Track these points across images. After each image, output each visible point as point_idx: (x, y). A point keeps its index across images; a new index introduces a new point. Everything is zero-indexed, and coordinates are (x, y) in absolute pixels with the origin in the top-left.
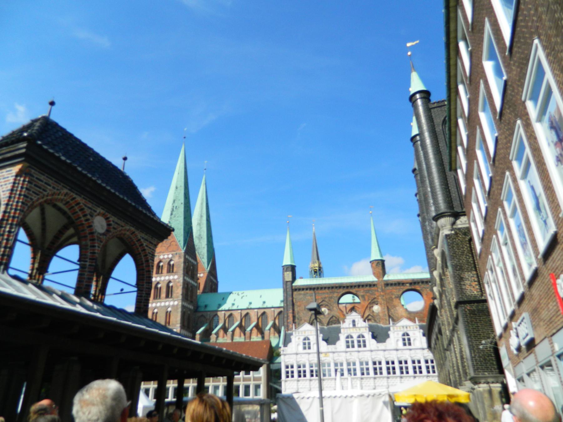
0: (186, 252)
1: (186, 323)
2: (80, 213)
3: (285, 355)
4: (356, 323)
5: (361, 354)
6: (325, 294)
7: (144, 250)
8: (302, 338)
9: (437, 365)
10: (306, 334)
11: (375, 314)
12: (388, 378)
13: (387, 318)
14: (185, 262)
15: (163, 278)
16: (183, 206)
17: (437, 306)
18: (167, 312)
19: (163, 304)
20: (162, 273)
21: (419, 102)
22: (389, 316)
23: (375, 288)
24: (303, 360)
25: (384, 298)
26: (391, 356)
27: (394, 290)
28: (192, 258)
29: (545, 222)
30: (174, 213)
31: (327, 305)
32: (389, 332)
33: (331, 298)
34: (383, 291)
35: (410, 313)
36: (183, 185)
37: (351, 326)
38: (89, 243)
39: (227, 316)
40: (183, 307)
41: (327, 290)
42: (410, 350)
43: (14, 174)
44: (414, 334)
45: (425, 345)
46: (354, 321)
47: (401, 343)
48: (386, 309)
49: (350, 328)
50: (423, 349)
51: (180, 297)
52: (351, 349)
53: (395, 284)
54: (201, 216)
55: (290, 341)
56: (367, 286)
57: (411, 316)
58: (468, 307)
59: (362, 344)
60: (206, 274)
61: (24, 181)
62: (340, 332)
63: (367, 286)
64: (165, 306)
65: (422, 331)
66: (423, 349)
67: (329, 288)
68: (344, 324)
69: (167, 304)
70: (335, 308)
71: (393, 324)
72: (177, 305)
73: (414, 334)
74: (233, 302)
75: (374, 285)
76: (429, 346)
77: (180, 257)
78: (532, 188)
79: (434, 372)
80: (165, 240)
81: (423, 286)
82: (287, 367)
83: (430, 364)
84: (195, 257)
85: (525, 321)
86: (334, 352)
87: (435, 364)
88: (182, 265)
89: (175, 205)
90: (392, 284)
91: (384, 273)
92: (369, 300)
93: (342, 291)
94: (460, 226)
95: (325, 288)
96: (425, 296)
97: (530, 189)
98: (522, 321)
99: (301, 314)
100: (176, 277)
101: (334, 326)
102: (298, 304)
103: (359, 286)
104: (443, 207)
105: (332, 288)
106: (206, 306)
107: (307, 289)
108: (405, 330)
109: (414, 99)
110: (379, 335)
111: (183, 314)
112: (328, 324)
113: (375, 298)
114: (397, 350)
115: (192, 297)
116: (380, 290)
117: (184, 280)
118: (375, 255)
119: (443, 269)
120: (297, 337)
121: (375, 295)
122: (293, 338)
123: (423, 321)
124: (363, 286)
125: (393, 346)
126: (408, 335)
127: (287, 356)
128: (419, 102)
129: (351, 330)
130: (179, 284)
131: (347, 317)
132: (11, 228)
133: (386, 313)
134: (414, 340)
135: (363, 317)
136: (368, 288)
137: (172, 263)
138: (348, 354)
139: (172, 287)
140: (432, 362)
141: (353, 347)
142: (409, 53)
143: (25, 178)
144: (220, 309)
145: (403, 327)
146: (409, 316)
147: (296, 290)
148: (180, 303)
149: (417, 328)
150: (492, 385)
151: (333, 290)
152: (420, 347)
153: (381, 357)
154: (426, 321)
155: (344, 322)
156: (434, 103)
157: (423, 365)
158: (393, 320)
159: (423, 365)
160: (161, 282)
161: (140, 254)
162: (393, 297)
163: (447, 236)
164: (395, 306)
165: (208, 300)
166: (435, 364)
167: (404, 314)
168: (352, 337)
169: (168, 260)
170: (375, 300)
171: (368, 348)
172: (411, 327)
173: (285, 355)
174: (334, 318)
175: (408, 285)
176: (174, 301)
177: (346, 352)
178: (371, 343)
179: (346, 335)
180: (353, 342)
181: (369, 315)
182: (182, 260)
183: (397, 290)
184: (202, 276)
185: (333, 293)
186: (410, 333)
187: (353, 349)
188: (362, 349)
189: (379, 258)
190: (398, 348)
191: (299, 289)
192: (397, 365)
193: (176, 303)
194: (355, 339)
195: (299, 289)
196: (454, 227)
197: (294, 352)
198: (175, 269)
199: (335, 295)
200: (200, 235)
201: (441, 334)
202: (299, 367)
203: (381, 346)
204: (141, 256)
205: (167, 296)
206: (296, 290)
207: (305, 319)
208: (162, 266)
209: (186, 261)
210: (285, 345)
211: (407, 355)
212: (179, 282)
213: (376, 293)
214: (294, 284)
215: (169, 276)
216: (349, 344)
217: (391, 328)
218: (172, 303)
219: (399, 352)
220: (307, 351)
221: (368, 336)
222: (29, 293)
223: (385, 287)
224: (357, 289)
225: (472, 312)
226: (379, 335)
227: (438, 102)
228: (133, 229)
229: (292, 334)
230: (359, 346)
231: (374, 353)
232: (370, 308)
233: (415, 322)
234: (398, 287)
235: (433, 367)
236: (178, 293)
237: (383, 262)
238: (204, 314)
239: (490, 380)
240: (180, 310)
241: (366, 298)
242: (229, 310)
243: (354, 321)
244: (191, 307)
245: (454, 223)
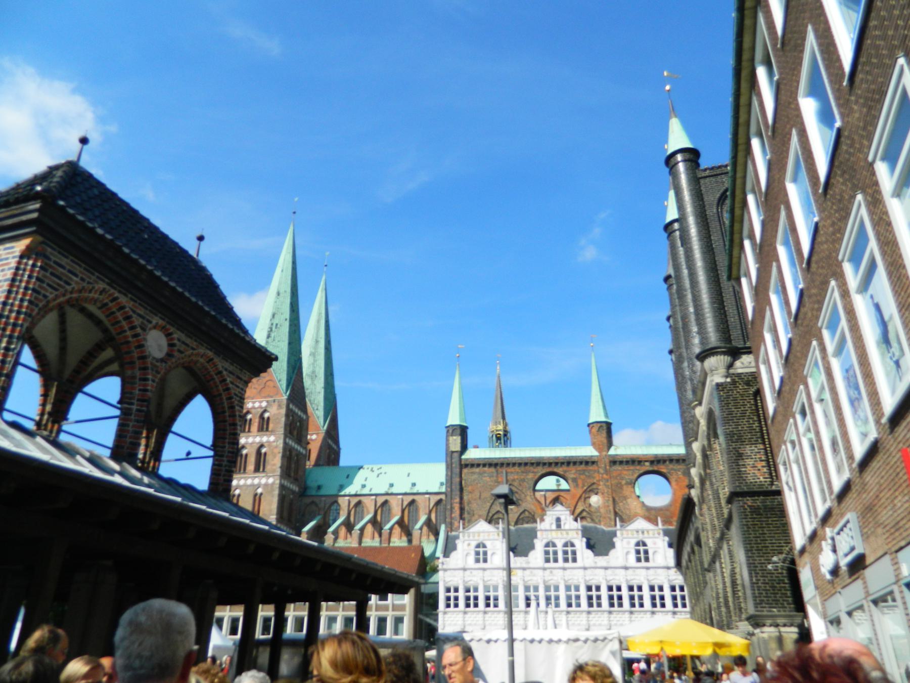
0: (291, 399)
1: (285, 514)
2: (124, 323)
3: (445, 570)
4: (562, 523)
5: (568, 572)
6: (515, 474)
7: (228, 389)
8: (474, 544)
9: (691, 594)
10: (481, 539)
11: (593, 510)
12: (610, 612)
13: (613, 517)
14: (287, 416)
15: (250, 440)
16: (287, 324)
17: (696, 500)
18: (256, 495)
19: (249, 482)
20: (249, 431)
21: (681, 167)
22: (616, 514)
23: (594, 467)
24: (475, 579)
25: (609, 484)
26: (617, 578)
27: (625, 472)
28: (300, 409)
29: (897, 363)
30: (272, 335)
32: (615, 540)
33: (523, 480)
34: (606, 472)
35: (649, 509)
36: (289, 290)
37: (554, 527)
38: (138, 373)
39: (352, 504)
40: (282, 487)
41: (516, 468)
42: (648, 568)
43: (18, 254)
44: (655, 544)
45: (671, 562)
46: (558, 520)
47: (632, 557)
48: (611, 503)
49: (551, 530)
50: (669, 568)
51: (278, 472)
52: (552, 564)
53: (627, 462)
54: (317, 342)
55: (454, 548)
56: (581, 463)
57: (651, 515)
58: (749, 501)
59: (571, 556)
60: (322, 436)
61: (34, 266)
62: (536, 537)
63: (581, 463)
64: (252, 485)
65: (667, 539)
66: (669, 568)
67: (520, 464)
68: (543, 524)
69: (256, 481)
70: (528, 498)
71: (621, 526)
72: (273, 483)
73: (655, 544)
74: (364, 483)
75: (593, 463)
76: (678, 564)
77: (280, 406)
78: (877, 307)
79: (684, 606)
80: (262, 375)
81: (671, 466)
82: (448, 590)
83: (678, 593)
84: (304, 409)
85: (849, 526)
86: (524, 569)
87: (686, 593)
88: (283, 419)
89: (275, 321)
90: (621, 462)
91: (610, 444)
92: (584, 486)
93: (541, 470)
94: (740, 371)
95: (514, 464)
96: (674, 483)
97: (873, 309)
98: (845, 526)
99: (474, 506)
100: (272, 438)
101: (526, 526)
102: (470, 488)
103: (568, 463)
104: (713, 338)
105: (526, 464)
106: (319, 487)
107: (484, 465)
108: (640, 537)
109: (672, 161)
110: (599, 543)
111: (282, 499)
112: (516, 523)
113: (594, 484)
114: (626, 568)
115: (296, 471)
116: (601, 471)
117: (285, 443)
118: (597, 414)
119: (709, 440)
120: (466, 543)
121: (594, 478)
122: (459, 544)
123: (670, 524)
124: (575, 463)
125: (620, 562)
126: (644, 544)
127: (448, 573)
128: (681, 167)
129: (554, 534)
130: (276, 451)
131: (548, 513)
132: (9, 343)
133: (611, 508)
134: (655, 553)
135: (573, 513)
136: (583, 467)
137: (266, 415)
138: (548, 572)
139: (265, 454)
140: (682, 589)
141: (556, 560)
142: (668, 88)
143: (36, 261)
144: (342, 493)
145: (637, 532)
146: (647, 514)
147: (466, 466)
148: (278, 482)
149: (659, 534)
150: (783, 629)
151: (527, 467)
152: (663, 564)
153: (600, 578)
154: (675, 523)
155: (542, 520)
156: (705, 170)
157: (667, 593)
158: (622, 520)
159: (667, 593)
160: (247, 446)
161: (220, 395)
162: (624, 482)
163: (718, 385)
164: (625, 498)
165: (322, 479)
166: (686, 593)
167: (639, 510)
168: (554, 545)
169: (260, 411)
170: (594, 487)
171: (580, 563)
172: (651, 532)
173: (445, 570)
174: (527, 513)
175: (647, 464)
176: (268, 477)
177: (545, 569)
178: (585, 556)
179: (545, 541)
180: (555, 553)
181: (583, 510)
182: (283, 411)
183: (630, 472)
184: (315, 438)
185: (527, 472)
186: (648, 541)
187: (555, 565)
189: (603, 419)
190: (628, 565)
191: (472, 465)
192: (625, 593)
193: (271, 480)
194: (560, 549)
195: (472, 465)
196: (731, 371)
197: (461, 565)
198: (271, 426)
199: (530, 476)
200: (314, 372)
201: (700, 545)
202: (468, 591)
203: (601, 561)
204: (221, 399)
205: (257, 469)
206: (466, 466)
207: (481, 513)
208: (251, 420)
209: (289, 413)
210: (446, 554)
211: (641, 577)
212: (276, 447)
213: (596, 475)
214: (463, 457)
215: (261, 436)
217: (618, 533)
218: (264, 481)
219: (630, 571)
220: (482, 565)
221: (580, 544)
222: (36, 450)
223: (610, 466)
224: (565, 468)
225: (755, 510)
226: (599, 543)
227: (712, 168)
228: (210, 354)
229: (457, 537)
230: (566, 560)
231: (589, 572)
232: (585, 499)
233: (657, 525)
234: (632, 468)
235: (683, 598)
236: (274, 465)
237: (609, 425)
238: (317, 500)
239: (780, 621)
240: (276, 492)
241: (580, 482)
242: (356, 495)
243: (558, 520)
244: (295, 488)
245: (730, 366)
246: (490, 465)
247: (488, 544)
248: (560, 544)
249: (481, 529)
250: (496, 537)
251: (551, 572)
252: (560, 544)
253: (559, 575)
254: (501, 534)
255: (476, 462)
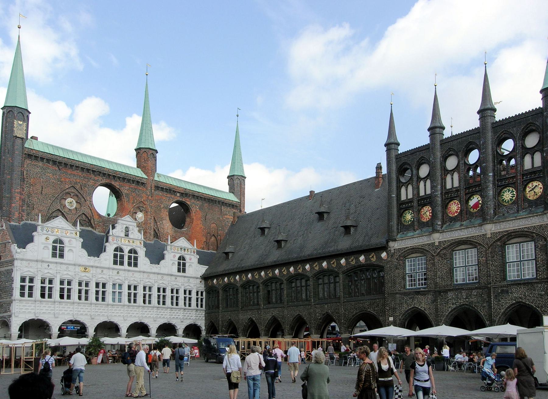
4: (130, 233)
8: (52, 239)
10: (59, 234)
31: (77, 196)
32: (165, 252)
37: (123, 235)
42: (185, 277)
46: (127, 230)
47: (176, 267)
50: (197, 278)
56: (133, 181)
59: (134, 262)
66: (197, 278)
67: (83, 169)
68: (114, 230)
75: (143, 184)
124: (129, 180)
131: (119, 221)
136: (133, 185)
140: (202, 295)
141: (122, 263)
145: (181, 249)
147: (29, 156)
153: (156, 282)
162: (162, 206)
164: (162, 219)
168: (121, 250)
175: (178, 195)
177: (114, 269)
179: (115, 246)
180: (122, 257)
187: (121, 267)
188: (132, 268)
203: (155, 268)
207: (41, 208)
216: (118, 259)
221: (141, 252)
230: (129, 264)
243: (127, 230)
246: (54, 162)
247: (66, 241)
248: (126, 250)
249: (60, 226)
250: (74, 235)
251: (118, 273)
252: (126, 250)
253: (126, 275)
254: (78, 233)
255: (40, 155)
